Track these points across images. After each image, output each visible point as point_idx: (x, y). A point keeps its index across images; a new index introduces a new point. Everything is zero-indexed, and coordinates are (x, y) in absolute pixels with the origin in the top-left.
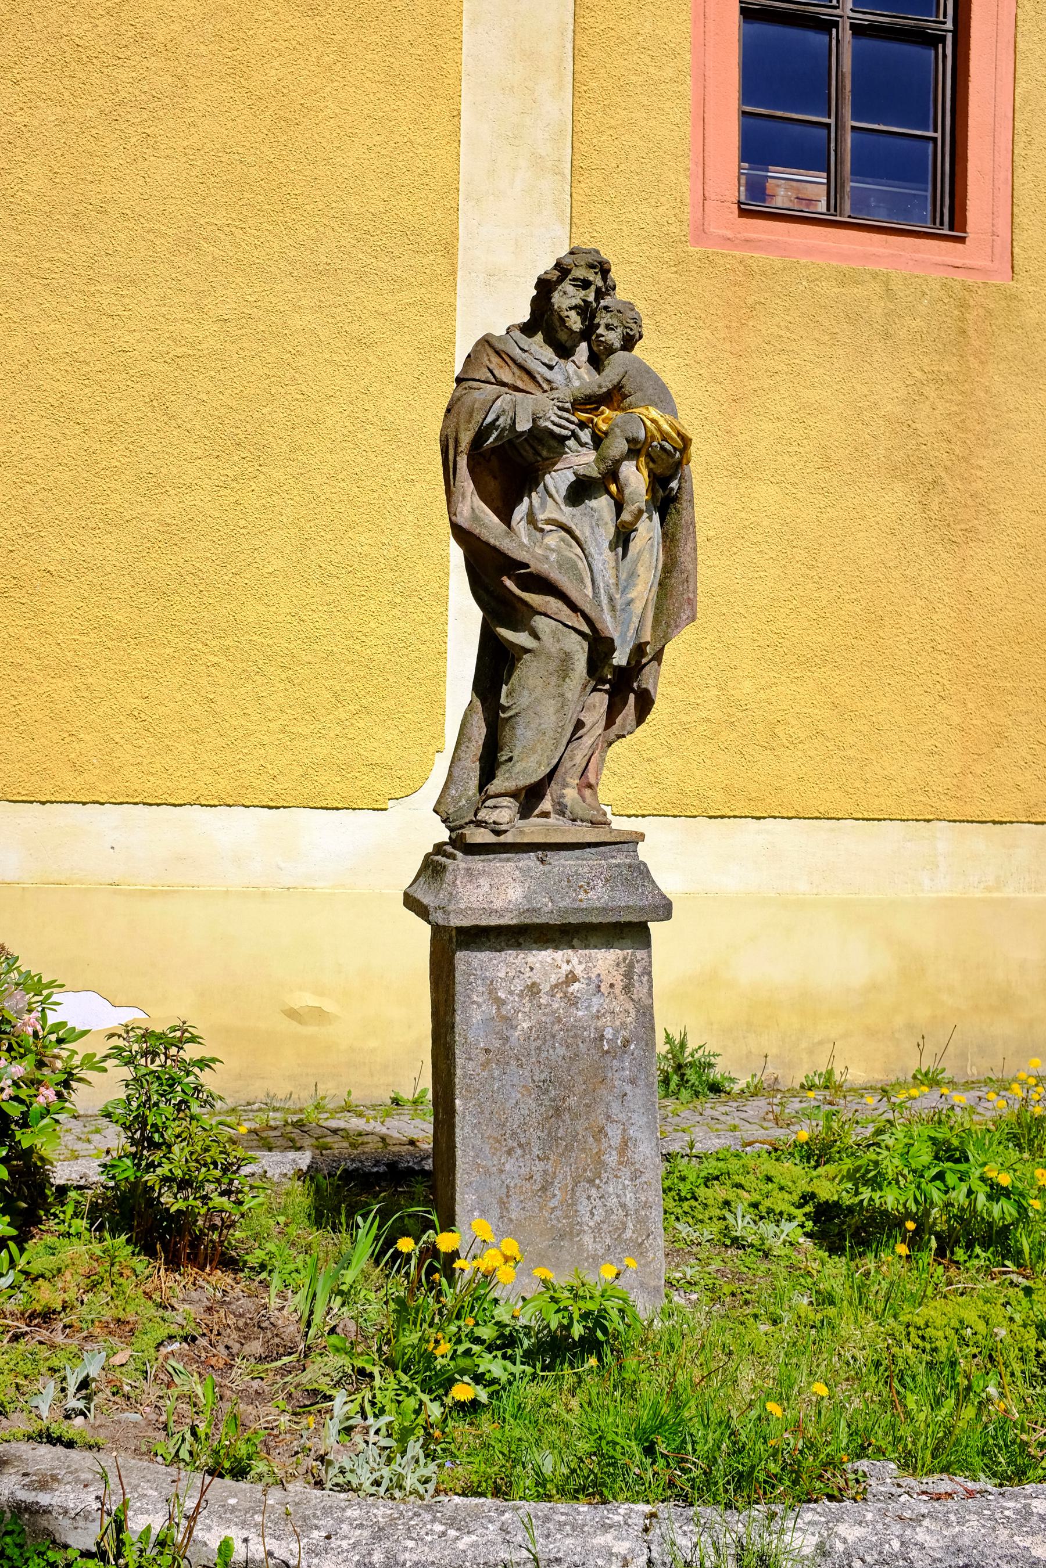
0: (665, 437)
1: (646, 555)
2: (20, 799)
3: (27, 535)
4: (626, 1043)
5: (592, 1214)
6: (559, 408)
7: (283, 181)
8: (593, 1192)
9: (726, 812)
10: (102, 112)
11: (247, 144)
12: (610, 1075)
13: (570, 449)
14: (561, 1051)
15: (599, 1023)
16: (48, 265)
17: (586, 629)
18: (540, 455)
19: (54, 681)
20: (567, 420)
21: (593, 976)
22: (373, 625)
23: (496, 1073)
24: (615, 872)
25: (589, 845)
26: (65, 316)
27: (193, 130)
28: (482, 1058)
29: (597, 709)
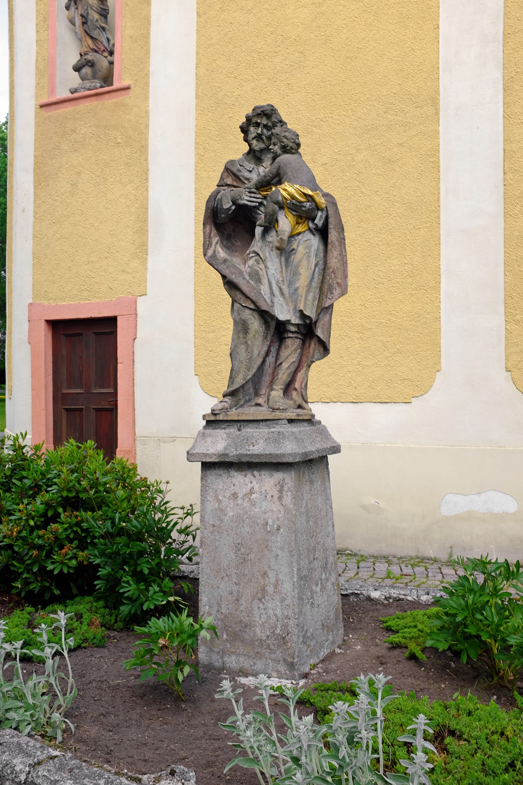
0: (293, 197)
1: (305, 263)
5: (260, 617)
7: (350, 88)
8: (261, 605)
10: (269, 79)
11: (332, 75)
12: (270, 544)
14: (247, 529)
15: (266, 516)
17: (252, 306)
20: (254, 197)
21: (263, 491)
22: (401, 307)
23: (217, 537)
24: (271, 435)
25: (262, 421)
27: (308, 76)
28: (211, 529)
29: (290, 348)
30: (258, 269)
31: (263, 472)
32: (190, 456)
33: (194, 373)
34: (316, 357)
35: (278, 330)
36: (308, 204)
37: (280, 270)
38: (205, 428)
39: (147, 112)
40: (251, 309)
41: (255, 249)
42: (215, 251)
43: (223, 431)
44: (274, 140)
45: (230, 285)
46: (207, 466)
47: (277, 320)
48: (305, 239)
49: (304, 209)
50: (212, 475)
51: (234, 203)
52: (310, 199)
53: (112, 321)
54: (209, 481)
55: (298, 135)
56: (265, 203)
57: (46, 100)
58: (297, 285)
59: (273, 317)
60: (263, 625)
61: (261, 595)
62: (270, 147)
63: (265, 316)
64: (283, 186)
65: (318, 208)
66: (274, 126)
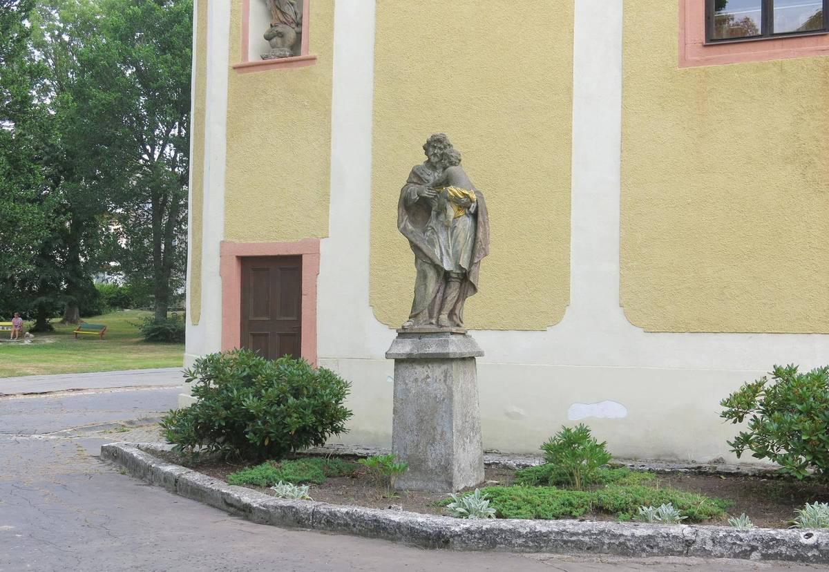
0: (456, 196)
4: (444, 400)
6: (429, 189)
9: (699, 330)
14: (424, 401)
17: (429, 262)
31: (435, 365)
32: (388, 356)
33: (368, 304)
35: (445, 277)
38: (397, 338)
39: (331, 81)
41: (431, 224)
45: (415, 248)
46: (399, 361)
47: (445, 270)
50: (402, 367)
53: (297, 259)
54: (400, 371)
56: (438, 196)
57: (240, 63)
59: (442, 268)
60: (433, 461)
61: (432, 442)
63: (437, 268)
64: (449, 188)
65: (472, 201)
66: (445, 147)
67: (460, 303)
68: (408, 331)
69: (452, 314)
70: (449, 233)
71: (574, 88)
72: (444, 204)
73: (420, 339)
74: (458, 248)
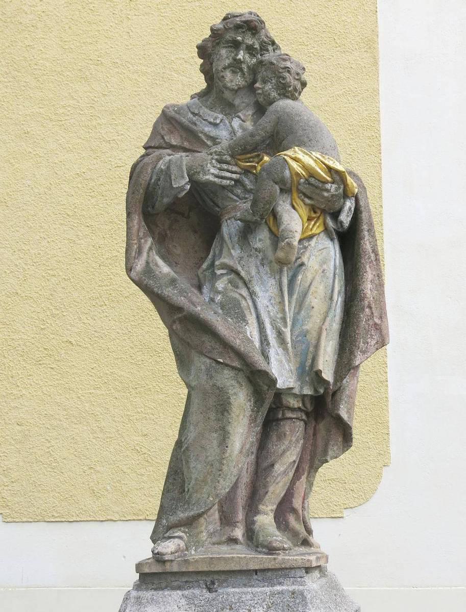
0: (311, 174)
2: (54, 520)
3: (53, 316)
6: (220, 161)
13: (238, 196)
16: (61, 111)
17: (236, 364)
18: (219, 207)
19: (77, 426)
25: (256, 571)
26: (76, 147)
30: (237, 296)
34: (330, 453)
36: (334, 186)
37: (278, 300)
38: (138, 587)
40: (233, 368)
42: (147, 263)
43: (179, 592)
44: (262, 73)
48: (321, 247)
49: (326, 194)
51: (191, 181)
52: (338, 178)
55: (304, 69)
58: (305, 327)
59: (274, 382)
62: (257, 85)
63: (257, 379)
64: (290, 152)
66: (264, 48)
67: (304, 478)
68: (175, 568)
69: (284, 509)
70: (285, 281)
71: (380, 40)
72: (271, 201)
73: (210, 590)
74: (307, 327)
